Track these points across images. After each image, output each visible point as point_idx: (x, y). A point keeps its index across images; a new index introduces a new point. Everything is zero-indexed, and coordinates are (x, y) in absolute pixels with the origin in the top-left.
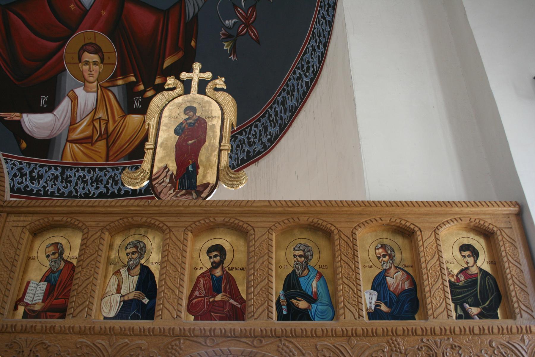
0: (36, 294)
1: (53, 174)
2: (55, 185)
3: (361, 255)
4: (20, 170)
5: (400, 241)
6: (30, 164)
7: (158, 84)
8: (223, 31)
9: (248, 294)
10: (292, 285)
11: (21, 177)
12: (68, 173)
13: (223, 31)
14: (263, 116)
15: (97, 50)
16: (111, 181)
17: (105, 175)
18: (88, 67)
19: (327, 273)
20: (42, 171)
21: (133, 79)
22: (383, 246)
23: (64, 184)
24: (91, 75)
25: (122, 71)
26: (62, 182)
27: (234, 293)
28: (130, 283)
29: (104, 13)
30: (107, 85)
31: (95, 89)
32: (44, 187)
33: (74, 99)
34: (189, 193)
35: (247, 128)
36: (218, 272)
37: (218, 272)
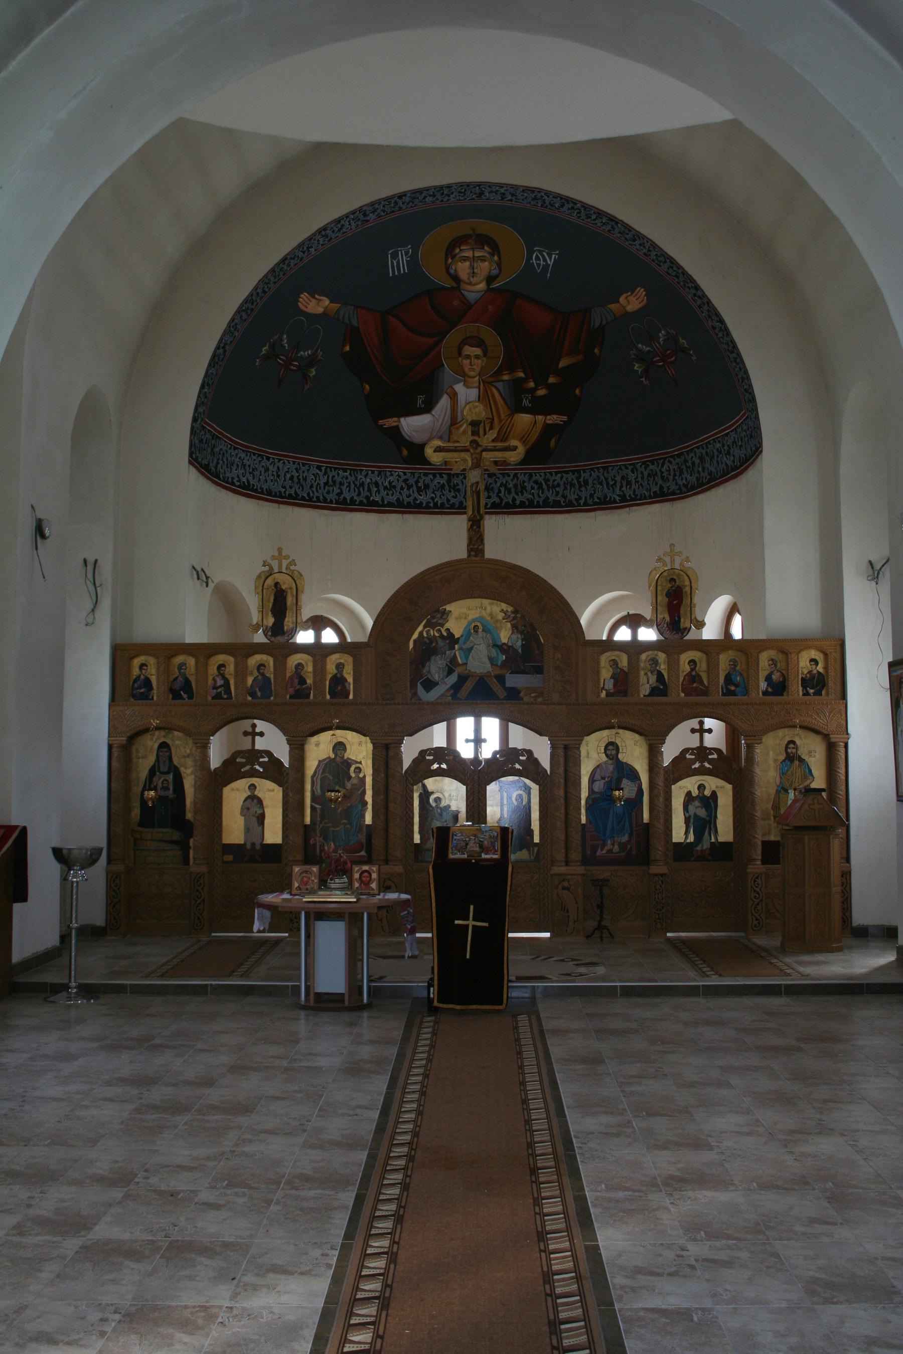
0: (610, 685)
1: (439, 483)
2: (443, 495)
3: (761, 664)
4: (405, 481)
5: (781, 656)
6: (413, 474)
7: (551, 384)
8: (634, 352)
9: (708, 682)
10: (728, 678)
11: (408, 489)
12: (455, 481)
13: (634, 352)
14: (679, 456)
15: (479, 343)
16: (503, 490)
17: (496, 482)
18: (468, 361)
19: (745, 674)
20: (428, 480)
21: (521, 375)
22: (772, 660)
23: (453, 494)
24: (473, 370)
25: (509, 365)
26: (450, 491)
27: (702, 683)
28: (653, 679)
29: (490, 308)
30: (491, 380)
31: (477, 385)
32: (432, 498)
33: (454, 396)
34: (677, 633)
35: (660, 459)
36: (694, 673)
37: (694, 673)
